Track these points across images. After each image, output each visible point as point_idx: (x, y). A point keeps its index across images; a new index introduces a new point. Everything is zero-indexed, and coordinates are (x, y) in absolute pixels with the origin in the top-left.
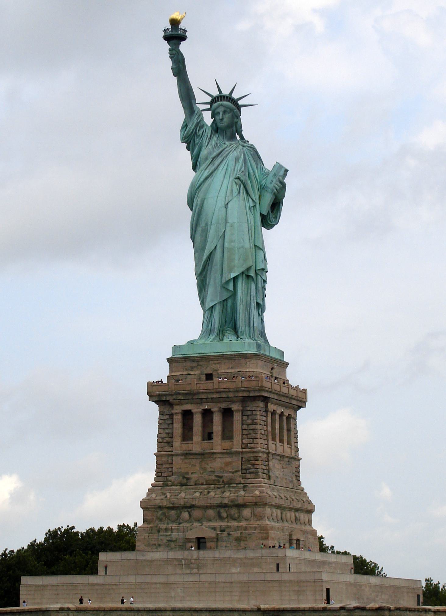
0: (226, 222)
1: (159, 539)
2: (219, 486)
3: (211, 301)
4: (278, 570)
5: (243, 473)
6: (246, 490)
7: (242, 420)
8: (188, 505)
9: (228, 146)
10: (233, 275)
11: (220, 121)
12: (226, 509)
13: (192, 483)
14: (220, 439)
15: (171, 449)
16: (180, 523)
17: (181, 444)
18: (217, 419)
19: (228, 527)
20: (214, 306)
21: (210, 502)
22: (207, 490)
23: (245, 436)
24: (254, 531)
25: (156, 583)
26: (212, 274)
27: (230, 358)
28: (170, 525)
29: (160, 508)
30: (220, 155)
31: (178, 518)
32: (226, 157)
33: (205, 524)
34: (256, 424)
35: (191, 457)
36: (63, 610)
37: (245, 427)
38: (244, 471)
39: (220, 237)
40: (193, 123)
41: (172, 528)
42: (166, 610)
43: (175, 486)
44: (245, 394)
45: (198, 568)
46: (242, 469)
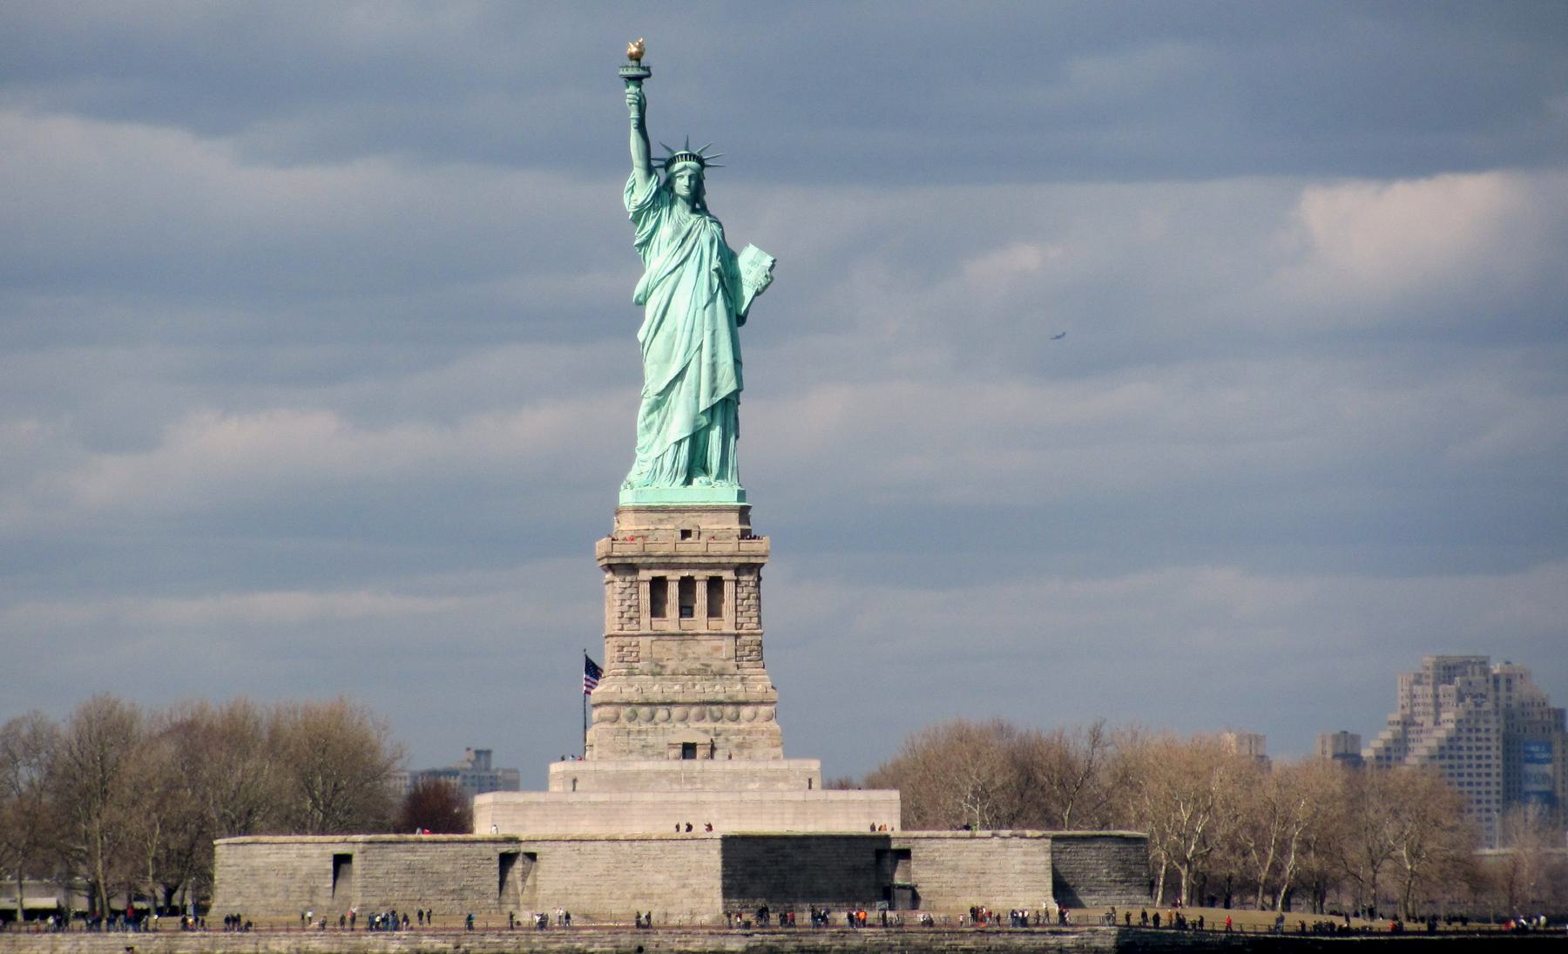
2: (707, 677)
3: (680, 432)
4: (810, 787)
8: (668, 701)
10: (716, 399)
12: (721, 707)
13: (669, 672)
15: (636, 627)
16: (656, 724)
19: (725, 731)
25: (682, 803)
28: (644, 726)
29: (629, 704)
30: (691, 235)
31: (653, 717)
33: (692, 725)
37: (739, 601)
44: (744, 560)
45: (703, 782)
46: (736, 656)
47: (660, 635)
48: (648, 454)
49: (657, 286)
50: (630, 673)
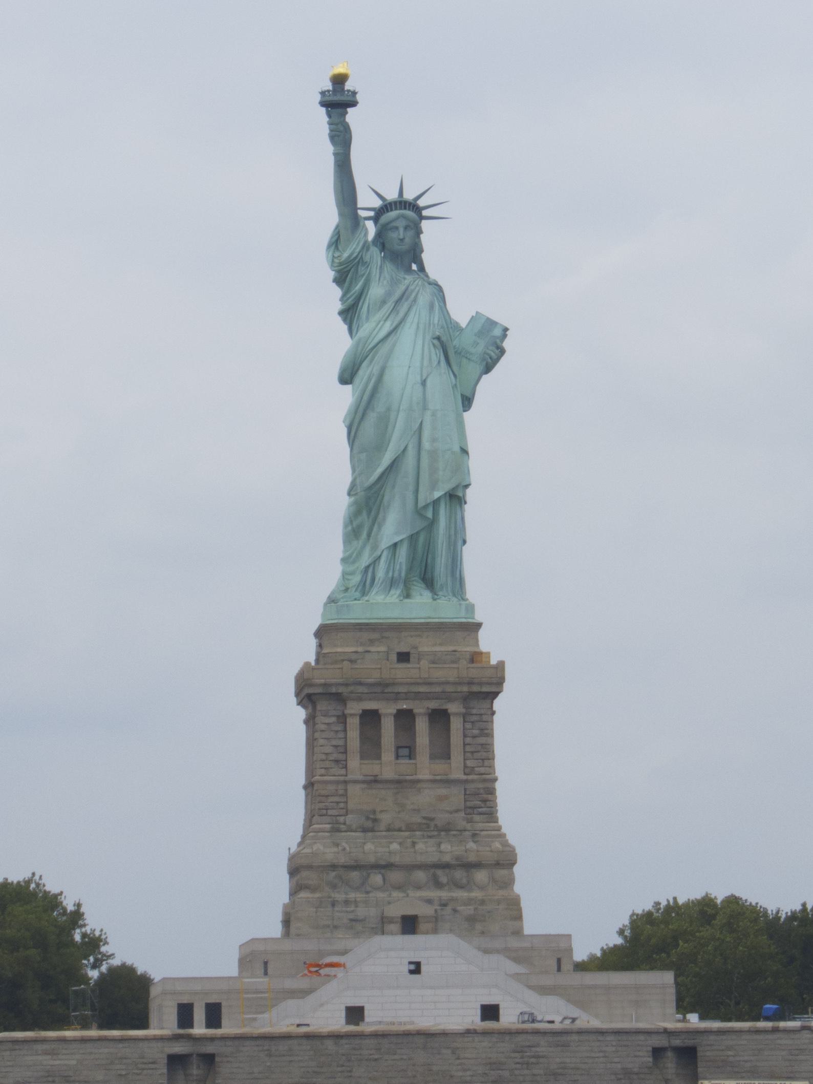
0: (425, 408)
2: (429, 834)
6: (478, 841)
8: (383, 863)
9: (412, 283)
10: (437, 494)
11: (399, 241)
12: (447, 871)
13: (382, 826)
15: (343, 772)
16: (367, 893)
17: (361, 764)
18: (422, 726)
19: (453, 899)
21: (420, 859)
22: (411, 840)
23: (469, 755)
24: (497, 907)
27: (438, 628)
28: (352, 895)
29: (334, 867)
30: (405, 297)
32: (415, 300)
33: (412, 893)
34: (487, 736)
35: (380, 786)
37: (468, 740)
38: (469, 811)
39: (413, 432)
40: (358, 243)
41: (358, 899)
42: (572, 1033)
43: (354, 832)
46: (466, 807)
47: (374, 781)
48: (357, 565)
49: (367, 356)
50: (335, 830)
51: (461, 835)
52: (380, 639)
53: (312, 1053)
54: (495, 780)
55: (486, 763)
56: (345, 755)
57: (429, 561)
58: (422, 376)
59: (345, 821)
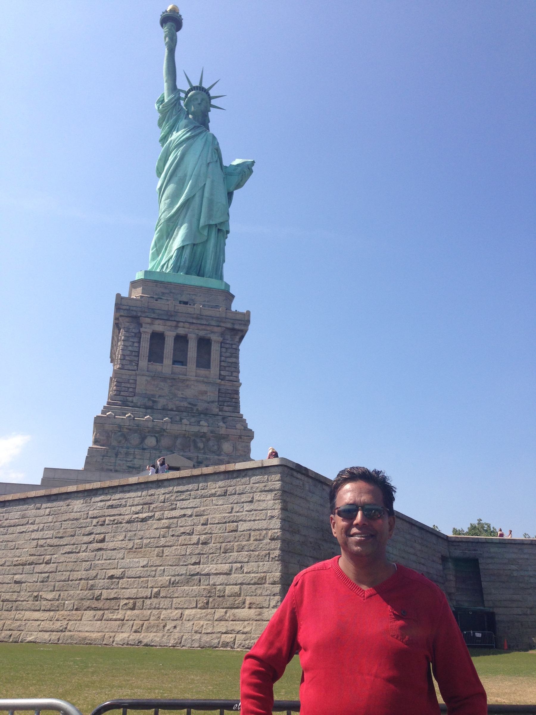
1: (117, 464)
2: (193, 414)
3: (183, 241)
5: (220, 405)
7: (221, 352)
10: (212, 223)
12: (204, 439)
13: (159, 406)
14: (195, 365)
16: (144, 449)
17: (148, 364)
19: (207, 459)
20: (186, 247)
23: (222, 368)
26: (187, 217)
28: (132, 451)
36: (298, 472)
37: (223, 358)
41: (135, 453)
46: (218, 401)
51: (215, 417)
52: (168, 293)
53: (50, 519)
54: (241, 384)
55: (234, 374)
56: (138, 358)
57: (203, 264)
58: (206, 161)
59: (133, 400)
